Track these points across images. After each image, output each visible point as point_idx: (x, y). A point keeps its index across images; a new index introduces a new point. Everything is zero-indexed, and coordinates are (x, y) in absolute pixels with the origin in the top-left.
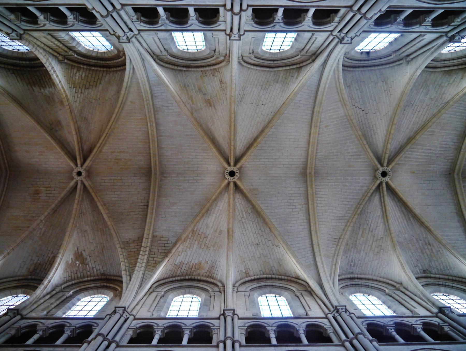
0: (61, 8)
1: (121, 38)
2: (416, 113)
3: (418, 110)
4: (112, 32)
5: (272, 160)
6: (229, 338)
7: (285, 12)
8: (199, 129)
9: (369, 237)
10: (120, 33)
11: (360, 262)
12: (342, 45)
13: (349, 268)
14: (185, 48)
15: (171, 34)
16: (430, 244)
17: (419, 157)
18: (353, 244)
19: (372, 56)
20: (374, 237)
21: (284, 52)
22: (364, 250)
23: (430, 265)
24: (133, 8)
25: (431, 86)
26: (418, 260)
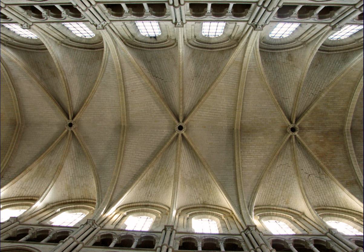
0: (56, 6)
1: (98, 26)
2: (202, 82)
3: (204, 80)
4: (92, 23)
5: (99, 116)
7: (213, 6)
8: (45, 93)
9: (165, 175)
10: (97, 22)
11: (155, 193)
12: (255, 31)
13: (146, 198)
14: (146, 34)
15: (135, 24)
16: (209, 182)
17: (208, 115)
18: (151, 180)
19: (159, 40)
20: (168, 175)
21: (219, 37)
22: (159, 185)
23: (208, 198)
24: (105, 5)
25: (211, 62)
26: (200, 194)
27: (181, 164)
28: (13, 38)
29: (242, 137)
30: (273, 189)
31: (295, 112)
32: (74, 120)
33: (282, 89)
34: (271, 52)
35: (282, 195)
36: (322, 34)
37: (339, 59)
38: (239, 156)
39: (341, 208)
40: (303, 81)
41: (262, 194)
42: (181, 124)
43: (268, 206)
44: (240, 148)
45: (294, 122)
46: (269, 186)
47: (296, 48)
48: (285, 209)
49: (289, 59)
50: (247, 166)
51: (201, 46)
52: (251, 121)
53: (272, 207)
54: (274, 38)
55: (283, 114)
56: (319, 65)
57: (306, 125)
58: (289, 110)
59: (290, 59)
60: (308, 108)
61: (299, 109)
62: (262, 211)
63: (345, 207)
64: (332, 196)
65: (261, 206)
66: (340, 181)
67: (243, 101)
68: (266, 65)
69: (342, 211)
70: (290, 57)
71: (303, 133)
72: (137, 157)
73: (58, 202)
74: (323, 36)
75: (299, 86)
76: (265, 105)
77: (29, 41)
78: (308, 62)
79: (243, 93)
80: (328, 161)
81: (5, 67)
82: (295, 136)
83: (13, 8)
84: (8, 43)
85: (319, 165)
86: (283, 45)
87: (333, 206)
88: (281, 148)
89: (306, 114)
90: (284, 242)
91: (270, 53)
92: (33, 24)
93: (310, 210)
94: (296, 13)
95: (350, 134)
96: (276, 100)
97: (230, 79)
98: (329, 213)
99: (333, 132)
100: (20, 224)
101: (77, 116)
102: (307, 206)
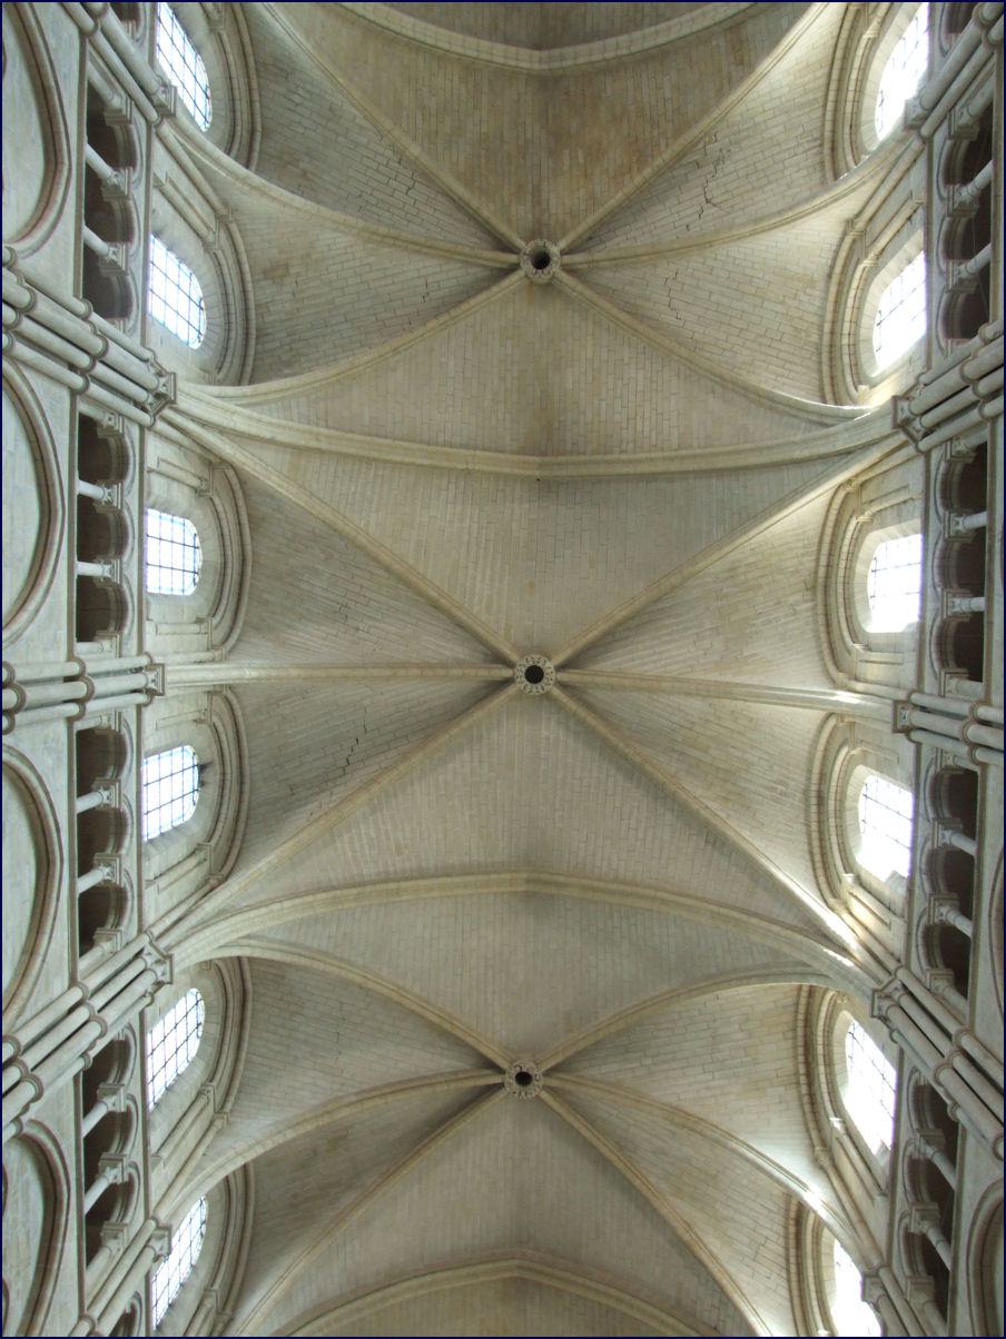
1: (161, 978)
3: (358, 589)
4: (148, 1000)
6: (963, 730)
8: (405, 1172)
9: (709, 733)
10: (146, 983)
11: (775, 767)
12: (178, 401)
14: (188, 801)
15: (151, 841)
16: (734, 569)
17: (488, 573)
18: (726, 781)
19: (211, 754)
20: (707, 721)
21: (200, 534)
22: (744, 752)
24: (82, 953)
25: (291, 561)
26: (778, 603)
27: (666, 672)
28: (206, 1290)
29: (569, 447)
30: (761, 336)
31: (477, 251)
32: (504, 1064)
33: (391, 300)
34: (257, 344)
35: (782, 303)
36: (190, 154)
37: (283, 90)
38: (639, 461)
39: (828, 84)
40: (361, 223)
41: (778, 375)
42: (520, 672)
43: (820, 354)
44: (608, 457)
45: (512, 258)
46: (747, 348)
47: (242, 248)
48: (833, 289)
49: (281, 277)
50: (675, 431)
51: (235, 600)
52: (508, 416)
53: (826, 338)
54: (203, 331)
55: (482, 297)
56: (302, 165)
57: (523, 212)
58: (468, 274)
59: (280, 272)
60: (461, 207)
61: (465, 237)
62: (838, 374)
63: (826, 70)
64: (784, 118)
65: (821, 380)
66: (730, 89)
67: (437, 444)
68: (303, 360)
69: (840, 80)
70: (275, 272)
71: (552, 222)
72: (641, 835)
73: (806, 1124)
74: (195, 153)
75: (379, 239)
76: (451, 364)
77: (217, 1229)
78: (291, 206)
79: (405, 444)
80: (656, 132)
81: (310, 1318)
82: (563, 253)
83: (95, 1293)
84: (224, 1308)
85: (669, 167)
86: (231, 297)
87: (819, 113)
88: (608, 306)
89: (485, 213)
90: (953, 293)
91: (259, 347)
92: (154, 1218)
93: (836, 200)
94: (112, 249)
95: (556, 52)
96: (432, 324)
97: (354, 493)
98: (847, 129)
99: (550, 115)
100: (888, 1265)
101: (490, 1055)
102: (819, 209)
